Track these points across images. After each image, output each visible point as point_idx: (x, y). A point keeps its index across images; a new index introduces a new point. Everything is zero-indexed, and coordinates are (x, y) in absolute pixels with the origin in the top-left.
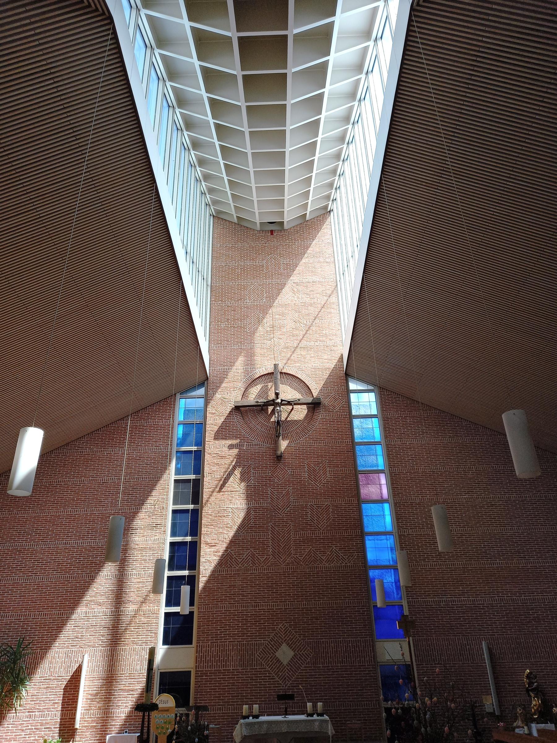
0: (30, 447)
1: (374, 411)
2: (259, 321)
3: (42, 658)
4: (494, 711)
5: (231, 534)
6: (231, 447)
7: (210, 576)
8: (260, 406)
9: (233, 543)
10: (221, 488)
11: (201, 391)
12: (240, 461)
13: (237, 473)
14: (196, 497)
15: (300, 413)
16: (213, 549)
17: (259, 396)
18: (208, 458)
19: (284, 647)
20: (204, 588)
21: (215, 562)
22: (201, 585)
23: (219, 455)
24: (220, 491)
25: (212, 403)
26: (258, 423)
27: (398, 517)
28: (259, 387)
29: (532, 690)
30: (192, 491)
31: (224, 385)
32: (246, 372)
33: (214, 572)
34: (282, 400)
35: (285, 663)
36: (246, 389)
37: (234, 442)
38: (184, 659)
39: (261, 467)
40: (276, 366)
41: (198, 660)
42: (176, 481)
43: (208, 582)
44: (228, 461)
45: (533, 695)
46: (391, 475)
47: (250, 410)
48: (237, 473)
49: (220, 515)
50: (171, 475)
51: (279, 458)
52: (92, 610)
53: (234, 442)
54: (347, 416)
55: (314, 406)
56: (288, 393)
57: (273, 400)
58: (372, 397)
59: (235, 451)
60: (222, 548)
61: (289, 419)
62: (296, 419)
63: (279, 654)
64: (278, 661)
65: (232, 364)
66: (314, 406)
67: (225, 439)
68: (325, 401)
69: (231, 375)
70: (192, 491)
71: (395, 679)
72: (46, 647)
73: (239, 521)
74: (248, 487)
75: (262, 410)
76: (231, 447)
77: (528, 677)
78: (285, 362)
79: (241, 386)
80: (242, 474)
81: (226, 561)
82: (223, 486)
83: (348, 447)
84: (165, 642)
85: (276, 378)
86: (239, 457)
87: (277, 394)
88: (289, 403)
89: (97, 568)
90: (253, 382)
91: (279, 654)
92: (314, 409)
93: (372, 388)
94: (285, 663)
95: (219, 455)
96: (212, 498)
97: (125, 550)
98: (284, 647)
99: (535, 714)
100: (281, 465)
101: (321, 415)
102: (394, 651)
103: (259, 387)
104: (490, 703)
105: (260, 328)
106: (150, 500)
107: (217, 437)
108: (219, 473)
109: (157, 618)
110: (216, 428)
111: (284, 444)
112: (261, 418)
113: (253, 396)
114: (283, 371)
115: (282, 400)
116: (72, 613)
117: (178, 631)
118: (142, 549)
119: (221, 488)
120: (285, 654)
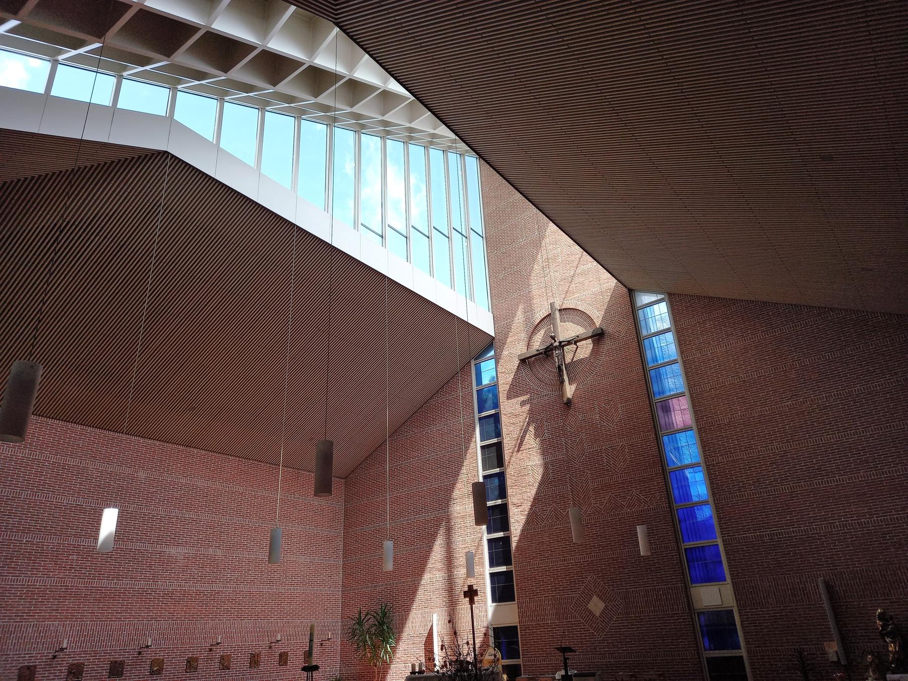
0: (109, 520)
1: (667, 324)
2: (534, 259)
3: (406, 619)
4: (839, 659)
5: (534, 492)
6: (523, 404)
7: (520, 536)
8: (541, 353)
9: (536, 500)
10: (519, 447)
11: (492, 353)
12: (533, 417)
13: (531, 429)
14: (500, 462)
15: (585, 349)
16: (520, 509)
17: (543, 341)
18: (504, 419)
19: (595, 599)
20: (517, 547)
21: (523, 521)
22: (514, 545)
23: (514, 413)
24: (518, 451)
25: (501, 361)
26: (546, 372)
27: (705, 446)
28: (542, 332)
29: (888, 634)
30: (495, 454)
31: (509, 340)
32: (527, 320)
33: (523, 531)
34: (560, 342)
35: (598, 615)
36: (530, 338)
37: (525, 398)
38: (510, 615)
39: (554, 420)
40: (552, 305)
41: (521, 615)
42: (482, 447)
43: (519, 541)
44: (522, 418)
45: (888, 640)
46: (691, 397)
47: (536, 360)
48: (531, 429)
49: (521, 474)
50: (478, 442)
51: (569, 403)
52: (433, 578)
53: (525, 398)
54: (637, 338)
55: (598, 336)
56: (568, 330)
57: (552, 344)
58: (662, 309)
59: (527, 407)
60: (527, 506)
61: (575, 359)
62: (582, 357)
63: (591, 606)
64: (591, 612)
65: (514, 315)
66: (598, 336)
67: (515, 397)
68: (609, 329)
69: (514, 326)
70: (495, 454)
71: (719, 627)
72: (408, 610)
73: (539, 478)
74: (542, 442)
75: (548, 356)
76: (523, 404)
77: (882, 617)
78: (563, 296)
79: (523, 336)
80: (536, 429)
81: (532, 518)
82: (521, 444)
83: (645, 374)
84: (494, 600)
85: (554, 319)
86: (531, 412)
87: (553, 338)
88: (569, 343)
89: (433, 537)
90: (536, 328)
91: (591, 606)
92: (599, 340)
93: (662, 296)
94: (598, 615)
95: (514, 413)
96: (513, 459)
97: (448, 520)
98: (595, 599)
99: (891, 663)
100: (571, 411)
101: (607, 345)
102: (712, 596)
103: (542, 332)
104: (833, 649)
105: (536, 267)
106: (464, 470)
107: (508, 398)
108: (516, 434)
109: (484, 579)
110: (507, 387)
111: (570, 390)
112: (548, 366)
113: (538, 343)
114: (564, 307)
115: (560, 342)
116: (421, 580)
117: (503, 590)
118: (463, 517)
119: (519, 447)
120: (596, 606)
